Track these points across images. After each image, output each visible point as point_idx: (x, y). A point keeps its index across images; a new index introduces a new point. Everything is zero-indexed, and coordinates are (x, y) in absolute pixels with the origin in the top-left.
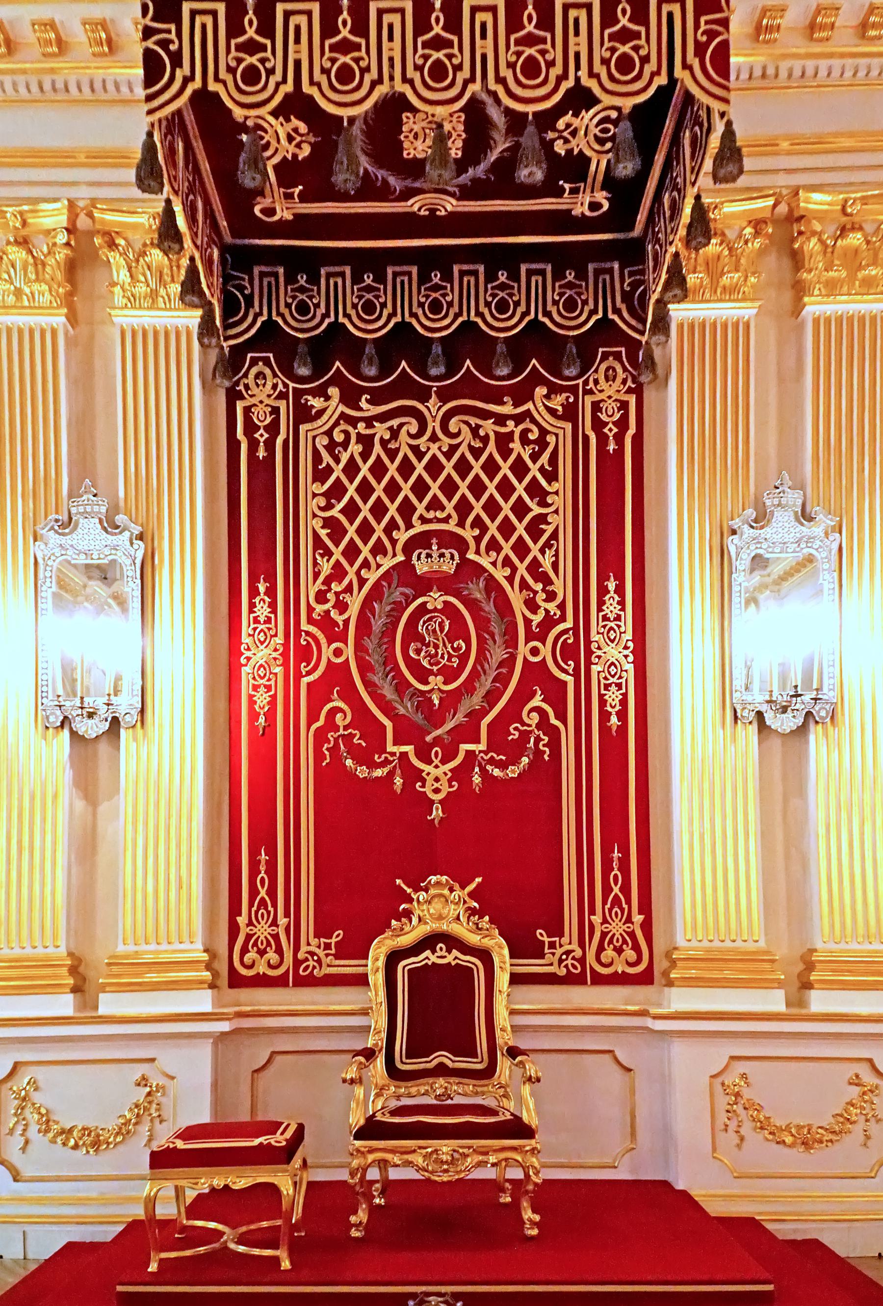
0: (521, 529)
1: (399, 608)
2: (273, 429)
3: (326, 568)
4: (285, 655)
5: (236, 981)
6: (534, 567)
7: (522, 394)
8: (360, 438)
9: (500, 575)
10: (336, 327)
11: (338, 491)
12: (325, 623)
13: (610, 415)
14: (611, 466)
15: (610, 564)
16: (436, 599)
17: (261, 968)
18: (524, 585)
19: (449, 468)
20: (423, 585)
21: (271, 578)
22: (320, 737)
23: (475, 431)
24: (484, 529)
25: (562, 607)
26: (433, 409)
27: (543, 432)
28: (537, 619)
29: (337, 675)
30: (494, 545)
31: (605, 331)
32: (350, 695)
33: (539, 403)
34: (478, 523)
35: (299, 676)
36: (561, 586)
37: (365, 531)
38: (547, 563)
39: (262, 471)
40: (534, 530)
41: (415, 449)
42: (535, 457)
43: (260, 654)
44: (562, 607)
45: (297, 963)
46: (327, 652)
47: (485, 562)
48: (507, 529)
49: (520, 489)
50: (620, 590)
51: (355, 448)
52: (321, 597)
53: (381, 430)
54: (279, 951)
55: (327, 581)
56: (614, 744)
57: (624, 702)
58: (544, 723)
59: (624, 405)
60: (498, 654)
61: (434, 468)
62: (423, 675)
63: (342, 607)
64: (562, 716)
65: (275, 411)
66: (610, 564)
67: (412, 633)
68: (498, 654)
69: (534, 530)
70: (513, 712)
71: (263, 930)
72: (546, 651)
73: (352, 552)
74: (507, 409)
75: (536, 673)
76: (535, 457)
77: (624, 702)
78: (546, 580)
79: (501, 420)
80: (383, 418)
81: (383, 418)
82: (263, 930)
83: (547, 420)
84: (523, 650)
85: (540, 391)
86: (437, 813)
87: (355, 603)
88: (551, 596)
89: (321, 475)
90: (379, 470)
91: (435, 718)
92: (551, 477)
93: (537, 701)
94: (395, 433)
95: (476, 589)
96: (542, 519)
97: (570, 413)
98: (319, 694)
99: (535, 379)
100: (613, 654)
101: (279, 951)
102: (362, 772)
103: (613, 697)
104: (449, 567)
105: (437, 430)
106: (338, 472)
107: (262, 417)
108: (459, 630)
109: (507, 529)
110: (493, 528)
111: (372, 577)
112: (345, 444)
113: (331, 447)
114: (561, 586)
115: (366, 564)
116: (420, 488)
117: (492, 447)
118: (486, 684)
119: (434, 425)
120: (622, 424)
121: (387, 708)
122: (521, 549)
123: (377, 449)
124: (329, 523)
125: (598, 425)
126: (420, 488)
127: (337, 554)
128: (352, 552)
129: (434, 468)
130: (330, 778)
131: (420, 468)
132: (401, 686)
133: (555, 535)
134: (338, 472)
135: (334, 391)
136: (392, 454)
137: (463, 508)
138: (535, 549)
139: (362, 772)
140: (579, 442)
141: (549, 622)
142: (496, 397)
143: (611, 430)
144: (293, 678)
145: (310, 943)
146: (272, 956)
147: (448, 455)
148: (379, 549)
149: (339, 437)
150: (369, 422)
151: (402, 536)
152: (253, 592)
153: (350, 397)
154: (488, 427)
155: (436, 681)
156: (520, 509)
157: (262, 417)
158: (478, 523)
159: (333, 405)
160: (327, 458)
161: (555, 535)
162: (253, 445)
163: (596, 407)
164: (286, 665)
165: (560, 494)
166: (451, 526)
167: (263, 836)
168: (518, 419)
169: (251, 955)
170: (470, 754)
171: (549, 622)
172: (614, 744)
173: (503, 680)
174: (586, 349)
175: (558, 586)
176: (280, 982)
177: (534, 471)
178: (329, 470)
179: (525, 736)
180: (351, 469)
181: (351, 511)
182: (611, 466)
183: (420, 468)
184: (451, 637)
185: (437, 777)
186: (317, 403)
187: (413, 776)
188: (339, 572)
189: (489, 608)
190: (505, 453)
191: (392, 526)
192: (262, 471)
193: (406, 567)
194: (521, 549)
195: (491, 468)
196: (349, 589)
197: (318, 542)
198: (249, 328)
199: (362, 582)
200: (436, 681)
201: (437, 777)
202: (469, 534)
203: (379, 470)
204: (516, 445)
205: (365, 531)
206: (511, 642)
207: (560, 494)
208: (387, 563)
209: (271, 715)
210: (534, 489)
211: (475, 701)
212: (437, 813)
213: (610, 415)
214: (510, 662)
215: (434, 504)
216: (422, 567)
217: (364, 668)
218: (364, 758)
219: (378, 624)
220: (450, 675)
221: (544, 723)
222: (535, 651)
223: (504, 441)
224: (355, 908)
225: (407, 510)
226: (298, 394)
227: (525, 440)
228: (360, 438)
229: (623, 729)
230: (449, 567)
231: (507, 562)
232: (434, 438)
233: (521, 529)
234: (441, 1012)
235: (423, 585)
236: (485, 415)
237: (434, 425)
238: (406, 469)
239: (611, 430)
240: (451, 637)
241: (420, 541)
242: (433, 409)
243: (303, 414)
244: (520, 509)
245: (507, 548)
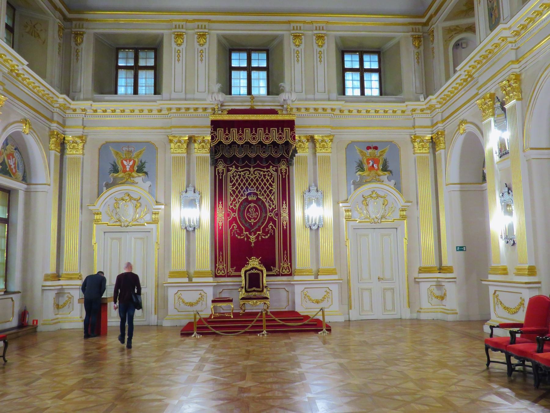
0: (268, 192)
1: (246, 207)
2: (223, 173)
3: (232, 199)
4: (225, 215)
5: (216, 276)
6: (270, 199)
7: (268, 167)
8: (239, 175)
9: (264, 200)
10: (234, 155)
11: (234, 185)
12: (232, 209)
13: (284, 171)
14: (284, 180)
15: (284, 198)
16: (252, 205)
17: (221, 274)
18: (268, 202)
19: (255, 180)
20: (250, 202)
21: (222, 201)
22: (231, 231)
23: (259, 174)
24: (261, 192)
25: (275, 206)
26: (252, 170)
27: (272, 174)
28: (271, 208)
29: (234, 219)
30: (263, 195)
31: (282, 156)
32: (237, 223)
33: (271, 169)
34: (260, 191)
35: (227, 219)
36: (275, 202)
37: (239, 192)
38: (273, 198)
39: (221, 181)
40: (270, 192)
41: (249, 177)
42: (270, 179)
43: (220, 215)
44: (275, 206)
45: (227, 273)
46: (233, 215)
47: (261, 198)
48: (265, 192)
49: (268, 184)
50: (286, 203)
51: (238, 177)
52: (231, 204)
53: (242, 173)
54: (224, 271)
55: (233, 201)
56: (285, 232)
57: (287, 224)
58: (272, 228)
59: (286, 169)
60: (264, 215)
61: (252, 180)
62: (250, 219)
63: (235, 206)
64: (276, 227)
65: (223, 170)
66: (284, 198)
67: (248, 211)
68: (264, 215)
69: (270, 192)
70: (267, 226)
71: (221, 267)
72: (272, 215)
73: (237, 196)
74: (265, 170)
75: (271, 219)
76: (270, 179)
77: (287, 224)
78: (273, 201)
79: (264, 172)
80: (243, 171)
81: (243, 171)
82: (221, 267)
83: (272, 172)
84: (268, 214)
85: (271, 167)
86: (253, 245)
87: (237, 205)
88: (273, 204)
89: (231, 182)
90: (242, 181)
91: (252, 227)
92: (273, 182)
93: (271, 224)
94: (245, 174)
95: (260, 203)
96: (272, 190)
97: (276, 171)
98: (231, 223)
99: (270, 164)
100: (285, 215)
101: (224, 271)
102: (239, 237)
103: (285, 223)
104: (255, 199)
105: (253, 173)
106: (234, 181)
107: (221, 171)
108: (256, 211)
109: (265, 192)
110: (263, 192)
111: (241, 201)
112: (236, 176)
113: (233, 176)
114: (275, 202)
115: (240, 198)
116: (249, 184)
117: (262, 177)
118: (262, 221)
119: (252, 172)
120: (286, 173)
121: (244, 226)
122: (268, 195)
123: (242, 177)
124: (233, 190)
125: (281, 173)
126: (249, 184)
127: (234, 196)
128: (237, 196)
129: (252, 180)
130: (233, 238)
131: (249, 180)
132: (246, 221)
133: (274, 193)
134: (234, 181)
135: (234, 166)
136: (244, 178)
137: (257, 188)
138: (270, 196)
139: (239, 237)
140: (278, 176)
141: (273, 209)
142: (263, 167)
143: (284, 174)
144: (226, 220)
145: (230, 269)
146: (223, 272)
147: (255, 178)
148: (242, 195)
149: (235, 175)
150: (240, 172)
151: (246, 193)
152: (219, 203)
153: (237, 167)
154: (262, 173)
155: (252, 220)
156: (268, 188)
157: (221, 171)
158: (260, 191)
159: (233, 169)
160: (232, 179)
161: (274, 193)
162: (219, 176)
163: (281, 170)
164: (225, 217)
165: (275, 185)
166: (255, 191)
167: (221, 249)
168: (267, 171)
169: (219, 271)
170: (259, 234)
171: (273, 209)
172: (285, 232)
173: (265, 220)
174: (279, 160)
175: (275, 202)
176: (224, 276)
177: (270, 181)
178: (233, 181)
179: (269, 230)
180: (237, 180)
181: (237, 188)
182: (284, 180)
183: (249, 180)
184: (255, 212)
185: (253, 238)
186: (231, 168)
187: (248, 238)
188: (234, 200)
189: (262, 206)
190: (265, 178)
191: (244, 191)
192: (221, 181)
193: (247, 199)
194: (268, 195)
195: (262, 180)
196: (236, 203)
197: (231, 194)
198: (219, 156)
199: (239, 201)
200: (252, 220)
201: (253, 238)
202: (258, 193)
203: (242, 181)
204: (267, 176)
205: (239, 192)
206: (266, 213)
207: (275, 185)
208: (243, 198)
209: (222, 227)
210: (270, 185)
211: (260, 224)
212: (253, 245)
213: (284, 171)
214: (266, 217)
215: (252, 187)
216: (250, 199)
217: (239, 218)
218: (239, 234)
219: (242, 209)
220: (255, 219)
221: (272, 228)
222: (270, 215)
223: (265, 176)
224: (238, 262)
225: (247, 188)
226: (227, 167)
227: (268, 176)
228: (239, 175)
229: (287, 229)
230: (255, 199)
231: (265, 198)
232: (252, 175)
233: (268, 192)
234: (254, 281)
235: (250, 202)
236: (261, 171)
237: (252, 172)
238: (247, 181)
239: (284, 174)
240: (255, 212)
241: (249, 194)
242: (252, 170)
243: (228, 171)
244: (268, 188)
245: (265, 195)
